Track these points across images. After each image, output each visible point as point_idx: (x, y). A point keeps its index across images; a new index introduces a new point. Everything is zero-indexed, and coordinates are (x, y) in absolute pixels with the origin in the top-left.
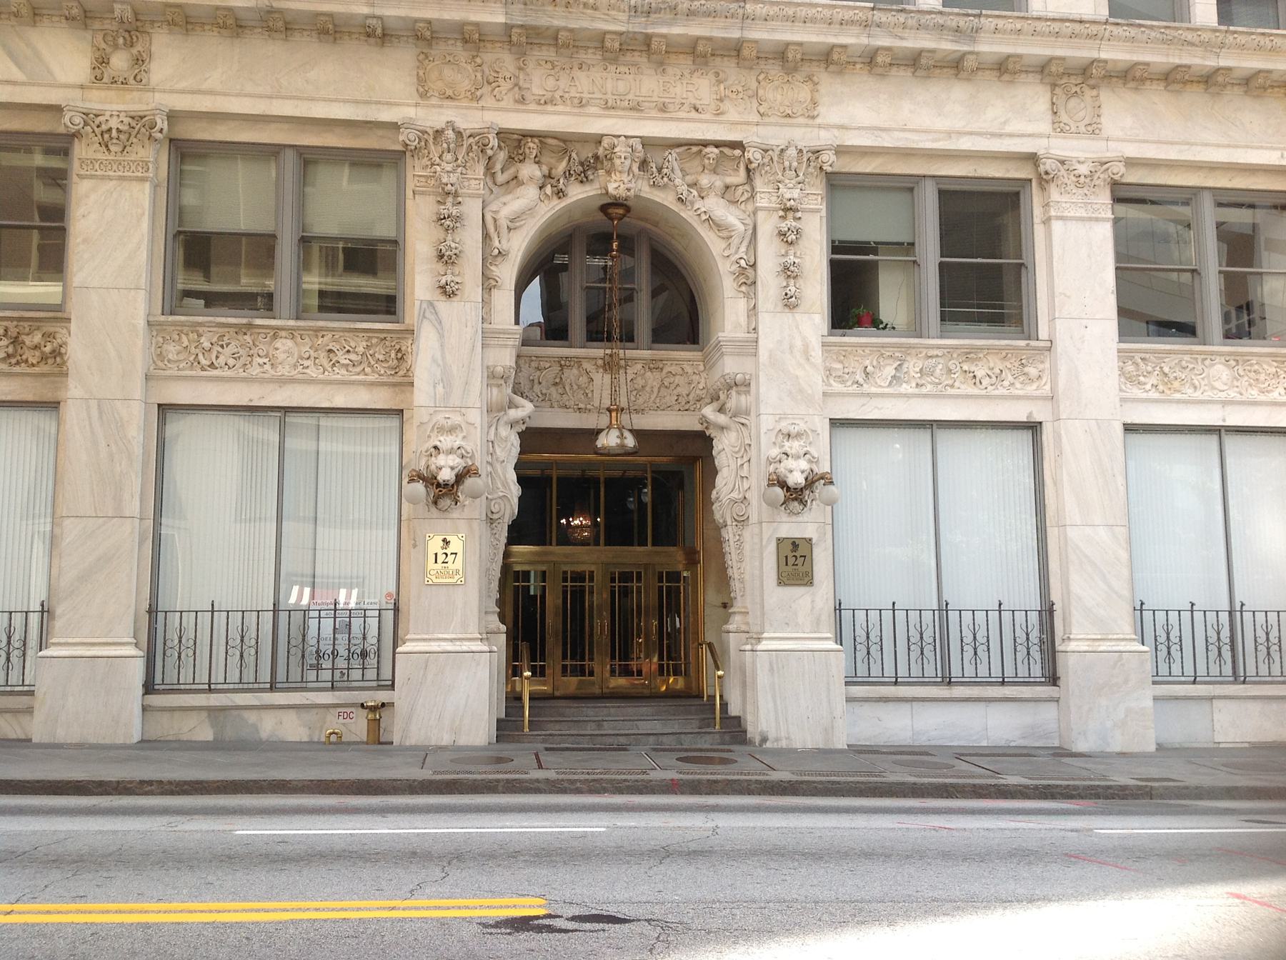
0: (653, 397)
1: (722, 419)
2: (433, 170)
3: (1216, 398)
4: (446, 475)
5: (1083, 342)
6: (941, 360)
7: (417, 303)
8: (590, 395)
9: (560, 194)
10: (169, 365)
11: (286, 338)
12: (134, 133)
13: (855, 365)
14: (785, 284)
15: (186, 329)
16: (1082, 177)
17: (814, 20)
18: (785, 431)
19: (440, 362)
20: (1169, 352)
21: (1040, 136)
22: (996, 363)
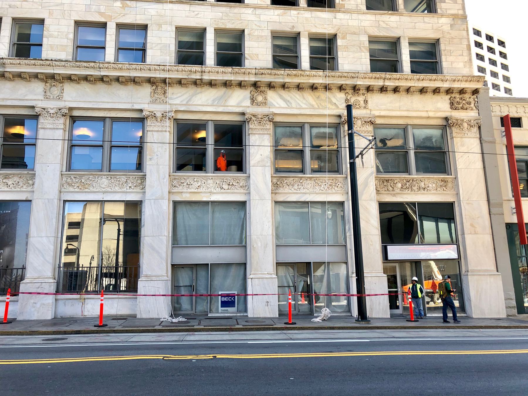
3: (101, 190)
5: (46, 171)
16: (52, 114)
22: (16, 179)
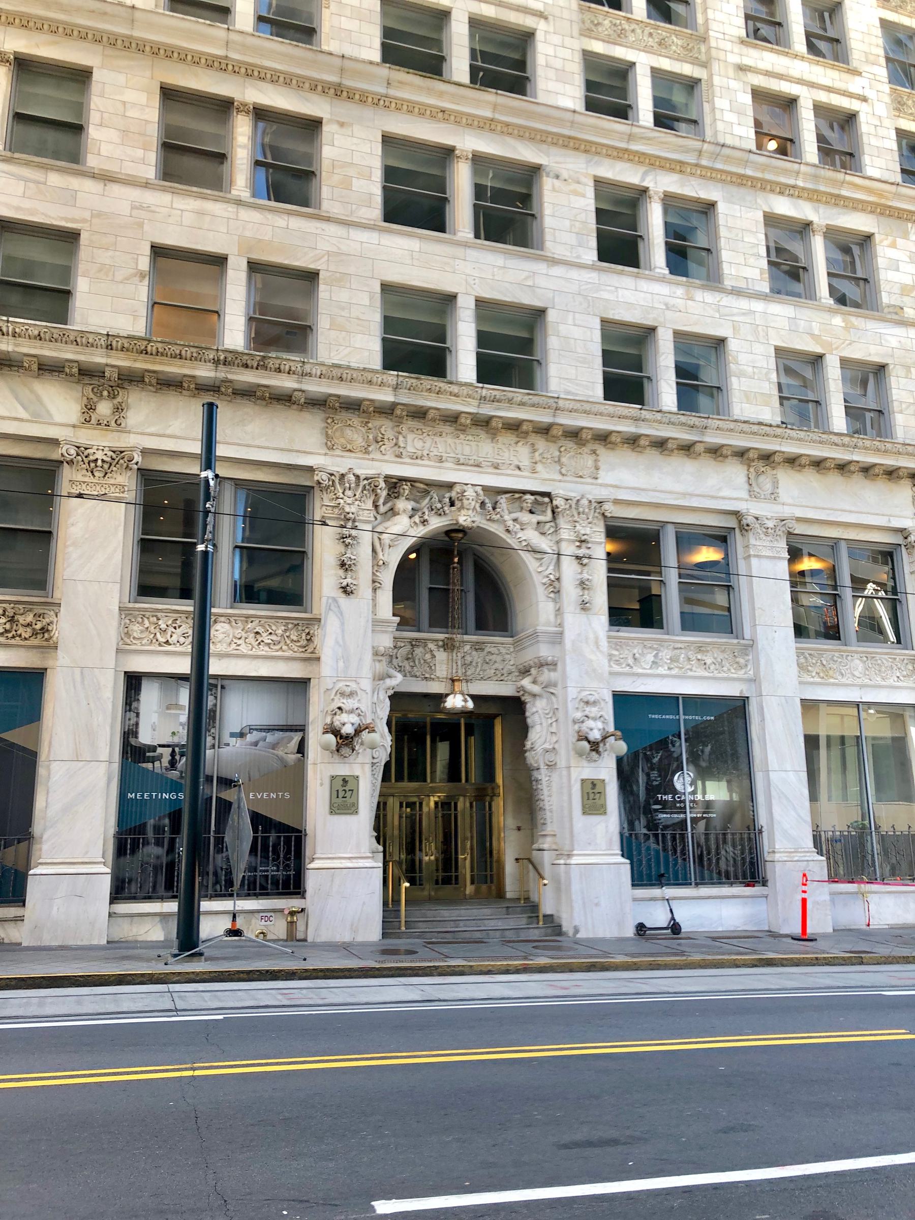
0: (478, 670)
1: (536, 689)
2: (337, 502)
3: (855, 682)
4: (348, 730)
6: (683, 651)
7: (324, 600)
8: (433, 668)
9: (424, 522)
10: (134, 642)
11: (224, 622)
12: (115, 463)
13: (626, 653)
14: (581, 594)
15: (147, 614)
17: (601, 414)
18: (585, 700)
19: (341, 643)
20: (826, 650)
21: (741, 499)
